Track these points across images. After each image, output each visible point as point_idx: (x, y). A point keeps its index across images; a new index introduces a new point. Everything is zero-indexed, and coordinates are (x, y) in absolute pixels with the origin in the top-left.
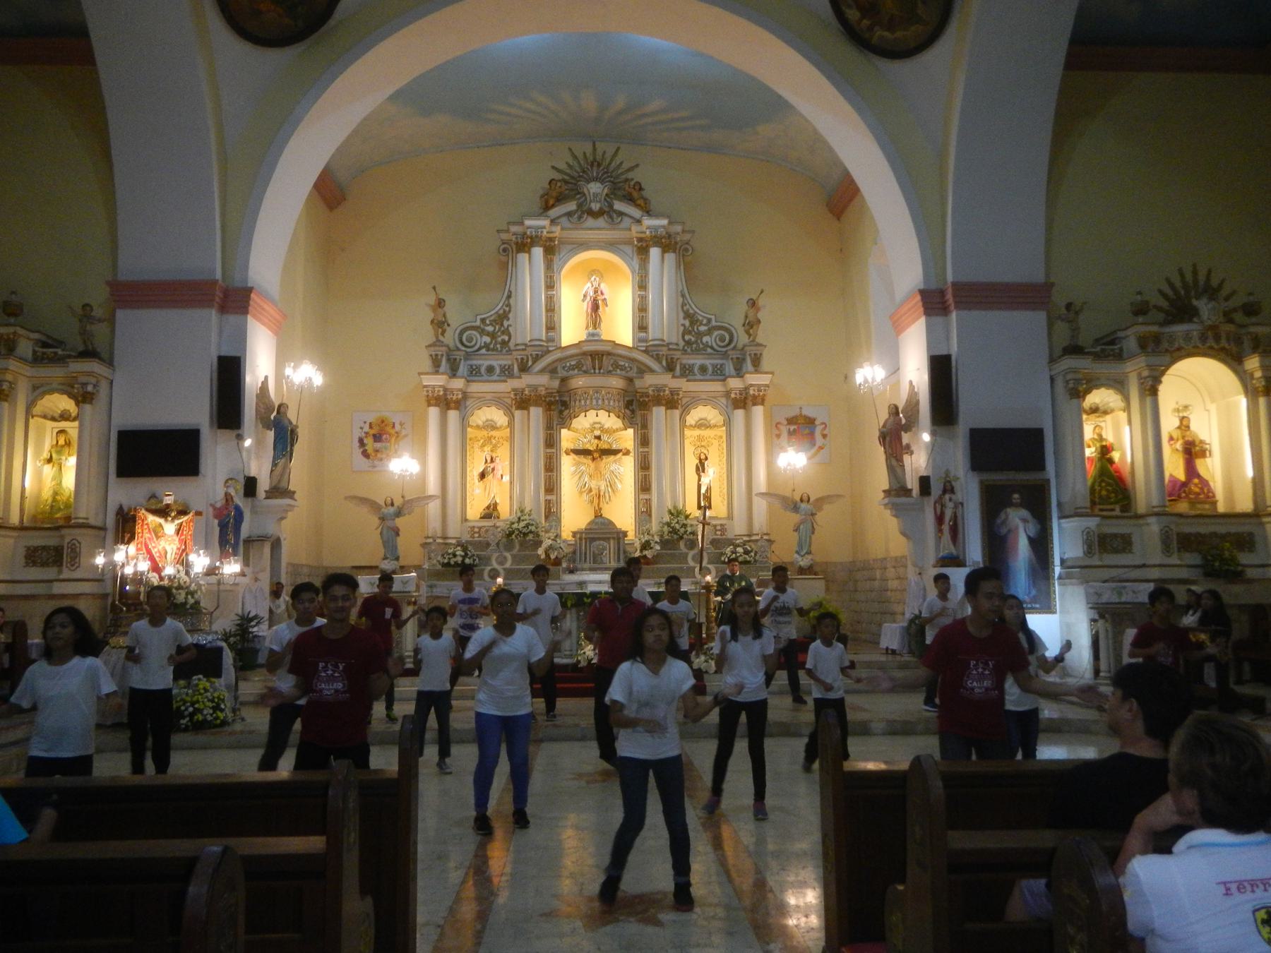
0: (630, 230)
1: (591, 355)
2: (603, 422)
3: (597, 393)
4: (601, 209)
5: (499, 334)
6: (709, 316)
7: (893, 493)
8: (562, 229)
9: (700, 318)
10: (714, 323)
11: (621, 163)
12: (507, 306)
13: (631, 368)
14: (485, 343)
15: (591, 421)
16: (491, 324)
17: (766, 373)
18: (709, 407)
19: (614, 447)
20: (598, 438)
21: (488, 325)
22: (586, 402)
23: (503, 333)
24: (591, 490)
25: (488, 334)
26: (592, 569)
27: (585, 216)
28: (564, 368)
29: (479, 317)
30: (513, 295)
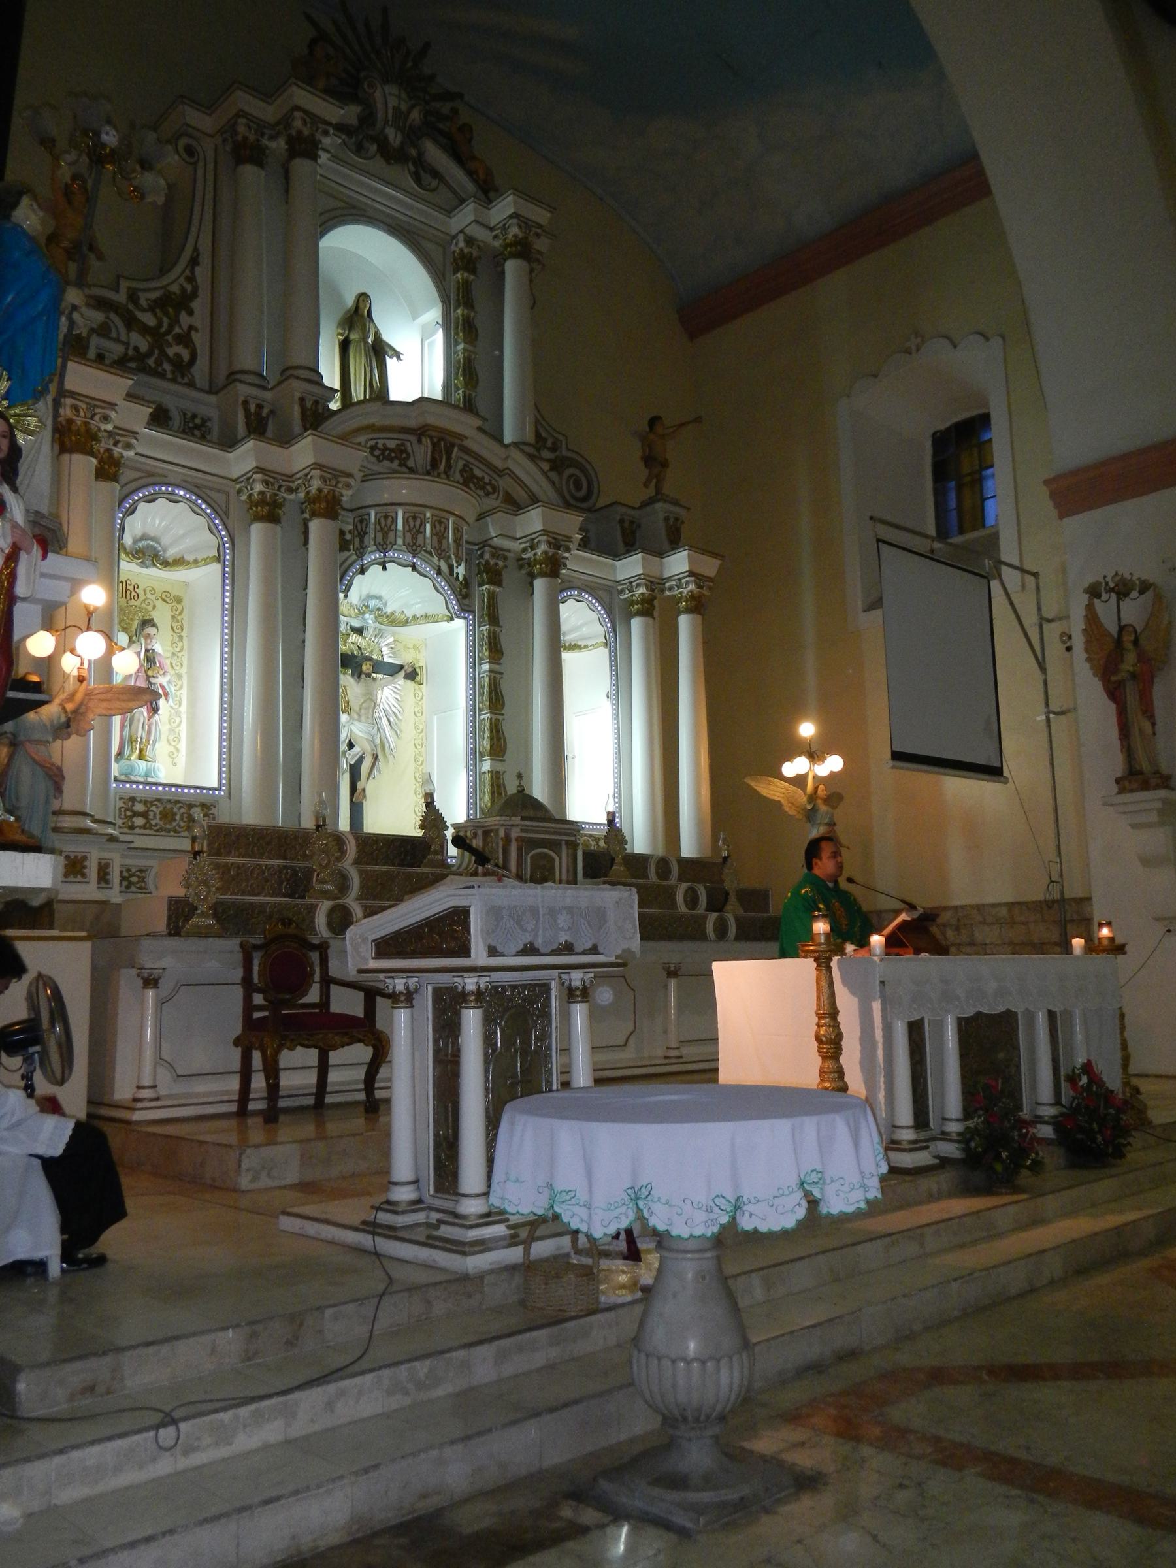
0: (449, 212)
1: (431, 438)
5: (169, 338)
6: (561, 437)
7: (1153, 781)
10: (565, 453)
13: (495, 490)
14: (136, 349)
15: (365, 592)
16: (152, 308)
17: (715, 555)
20: (359, 631)
21: (143, 310)
25: (145, 330)
29: (124, 285)
30: (205, 259)
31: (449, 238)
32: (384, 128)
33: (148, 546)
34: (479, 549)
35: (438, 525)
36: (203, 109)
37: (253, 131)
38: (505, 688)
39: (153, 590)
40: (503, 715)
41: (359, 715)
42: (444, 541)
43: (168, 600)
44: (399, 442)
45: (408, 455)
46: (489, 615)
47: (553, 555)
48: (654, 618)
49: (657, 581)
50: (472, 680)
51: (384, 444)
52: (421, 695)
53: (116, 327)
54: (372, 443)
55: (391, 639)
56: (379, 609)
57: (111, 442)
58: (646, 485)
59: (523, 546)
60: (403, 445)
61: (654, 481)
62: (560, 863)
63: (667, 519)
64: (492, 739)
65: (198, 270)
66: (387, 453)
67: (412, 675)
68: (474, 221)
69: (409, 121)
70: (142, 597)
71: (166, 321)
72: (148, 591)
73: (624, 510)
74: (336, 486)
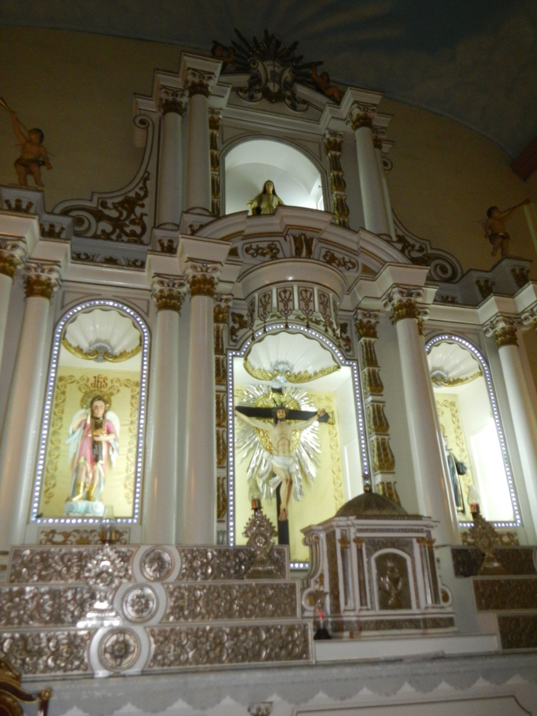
0: (318, 121)
2: (291, 361)
3: (306, 291)
4: (280, 92)
5: (127, 222)
8: (229, 104)
9: (412, 242)
10: (430, 251)
11: (301, 58)
12: (141, 189)
14: (103, 231)
15: (273, 360)
18: (455, 346)
19: (305, 408)
21: (110, 209)
22: (286, 305)
23: (133, 222)
24: (273, 475)
26: (379, 625)
27: (260, 95)
28: (247, 250)
31: (321, 137)
32: (266, 84)
33: (100, 348)
34: (355, 314)
35: (304, 294)
36: (148, 98)
37: (170, 95)
38: (388, 412)
39: (118, 380)
40: (388, 435)
41: (278, 451)
42: (311, 304)
43: (130, 386)
44: (270, 243)
45: (278, 250)
46: (368, 360)
47: (407, 302)
48: (518, 345)
49: (515, 316)
50: (361, 412)
51: (257, 246)
52: (334, 432)
53: (86, 217)
54: (248, 245)
55: (305, 394)
56: (287, 371)
57: (39, 270)
58: (493, 254)
59: (384, 302)
60: (273, 244)
61: (500, 250)
62: (413, 563)
63: (513, 271)
64: (379, 455)
65: (148, 183)
66: (260, 251)
67: (324, 418)
68: (333, 118)
69: (283, 78)
70: (110, 385)
71: (125, 213)
72: (114, 381)
73: (479, 274)
74: (206, 271)
